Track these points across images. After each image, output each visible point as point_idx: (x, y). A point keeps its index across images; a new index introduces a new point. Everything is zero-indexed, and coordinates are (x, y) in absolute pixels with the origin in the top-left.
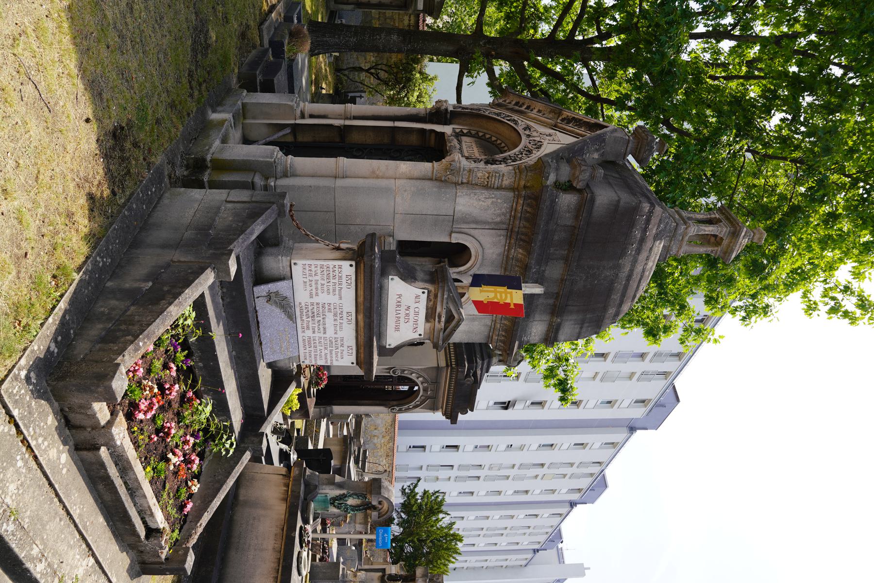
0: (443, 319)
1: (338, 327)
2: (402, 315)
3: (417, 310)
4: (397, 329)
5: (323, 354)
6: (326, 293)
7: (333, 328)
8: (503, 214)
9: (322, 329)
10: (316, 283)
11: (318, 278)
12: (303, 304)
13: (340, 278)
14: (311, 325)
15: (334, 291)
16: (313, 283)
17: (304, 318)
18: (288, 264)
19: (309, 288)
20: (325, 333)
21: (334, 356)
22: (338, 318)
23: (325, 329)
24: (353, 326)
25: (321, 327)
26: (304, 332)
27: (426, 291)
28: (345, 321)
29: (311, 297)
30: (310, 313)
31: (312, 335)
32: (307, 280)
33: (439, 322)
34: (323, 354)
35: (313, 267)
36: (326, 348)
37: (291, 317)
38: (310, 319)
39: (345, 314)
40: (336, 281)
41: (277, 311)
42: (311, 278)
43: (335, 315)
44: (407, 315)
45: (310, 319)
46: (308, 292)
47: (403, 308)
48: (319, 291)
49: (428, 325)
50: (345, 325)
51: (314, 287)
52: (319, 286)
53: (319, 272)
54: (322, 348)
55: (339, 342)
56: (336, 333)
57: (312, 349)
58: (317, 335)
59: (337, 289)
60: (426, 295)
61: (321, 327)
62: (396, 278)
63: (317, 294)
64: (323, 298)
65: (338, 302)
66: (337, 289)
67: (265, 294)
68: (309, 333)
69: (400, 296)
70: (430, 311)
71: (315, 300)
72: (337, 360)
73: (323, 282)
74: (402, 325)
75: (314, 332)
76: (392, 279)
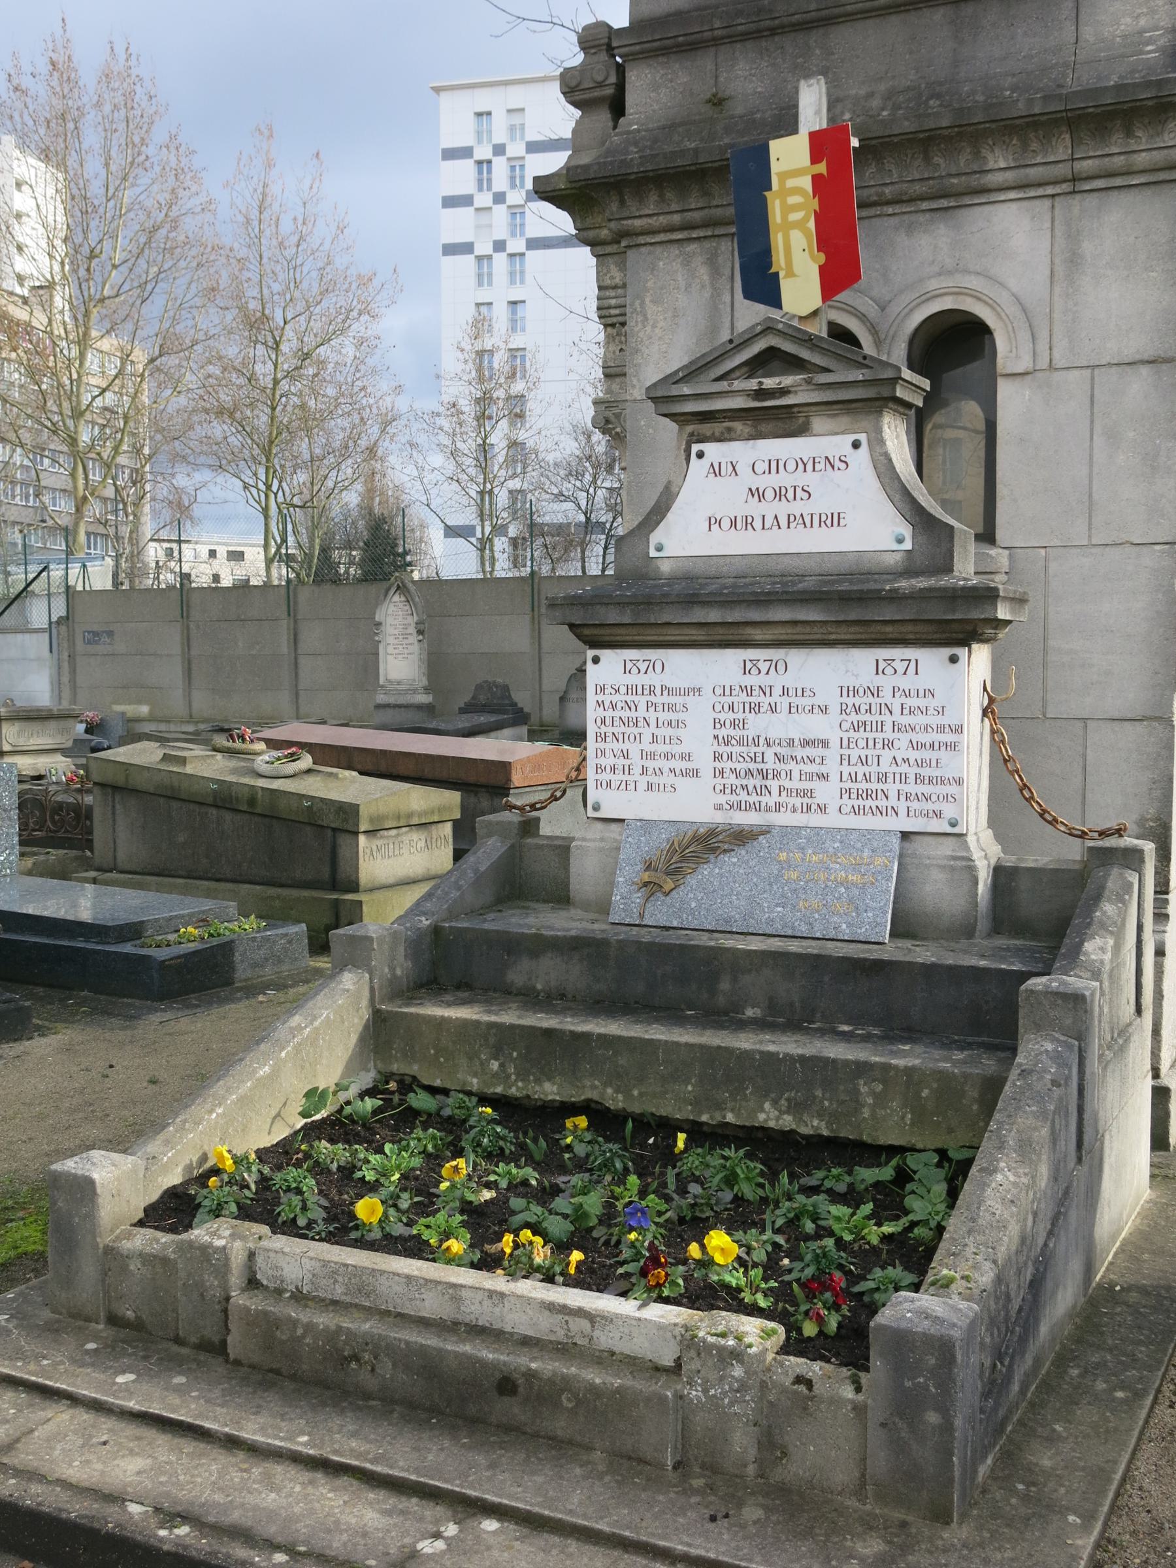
0: (770, 383)
1: (799, 700)
2: (782, 509)
3: (761, 467)
4: (835, 520)
5: (913, 755)
6: (680, 732)
7: (804, 718)
8: (687, 263)
9: (809, 751)
10: (652, 756)
11: (634, 749)
12: (722, 799)
13: (632, 690)
14: (795, 784)
15: (672, 708)
16: (650, 764)
17: (769, 800)
18: (599, 825)
19: (668, 779)
20: (825, 744)
21: (919, 720)
22: (765, 701)
23: (806, 743)
24: (795, 657)
25: (800, 753)
26: (822, 809)
27: (695, 448)
28: (777, 680)
29: (696, 773)
30: (751, 782)
31: (834, 785)
32: (642, 782)
33: (784, 392)
34: (913, 755)
35: (602, 761)
36: (889, 744)
37: (742, 837)
38: (773, 785)
39: (752, 680)
40: (642, 701)
41: (708, 873)
42: (637, 770)
43: (755, 708)
44: (779, 494)
45: (773, 785)
46: (680, 782)
47: (755, 508)
48: (676, 749)
49: (817, 423)
50: (789, 680)
51: (666, 765)
52: (660, 748)
53: (617, 746)
54: (887, 755)
55: (862, 701)
56: (824, 710)
57: (892, 788)
58: (832, 767)
59: (666, 699)
60: (707, 447)
61: (800, 753)
62: (655, 537)
63: (687, 757)
64: (698, 737)
65: (708, 698)
66: (666, 699)
67: (638, 898)
68: (826, 793)
69: (713, 522)
70: (764, 427)
71: (704, 761)
72: (941, 711)
73: (647, 738)
74: (820, 505)
75: (824, 777)
76: (659, 548)
